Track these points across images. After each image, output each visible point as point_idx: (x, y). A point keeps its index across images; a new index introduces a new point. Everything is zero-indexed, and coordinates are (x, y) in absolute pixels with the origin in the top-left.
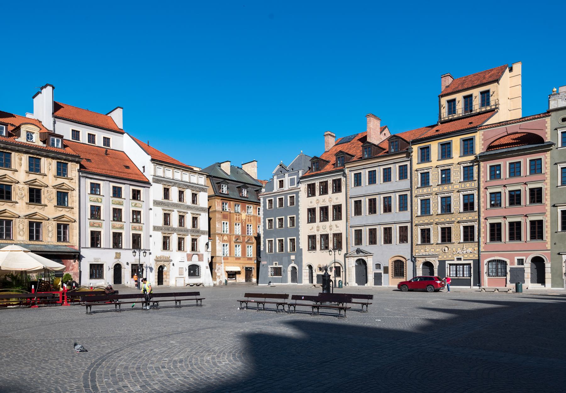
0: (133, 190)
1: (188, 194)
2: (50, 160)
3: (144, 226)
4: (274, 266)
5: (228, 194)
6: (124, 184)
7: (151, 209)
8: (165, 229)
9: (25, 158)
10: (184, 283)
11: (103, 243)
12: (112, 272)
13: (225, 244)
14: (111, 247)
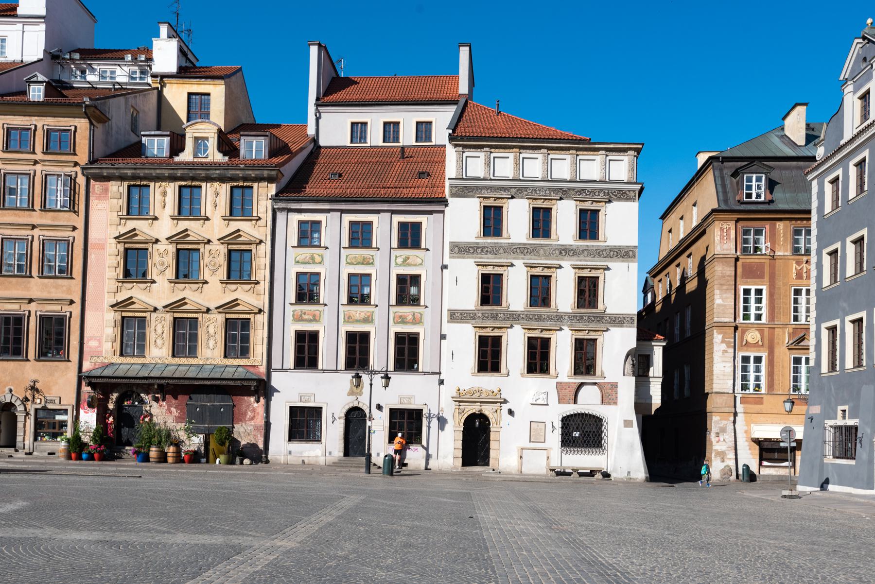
0: (403, 226)
1: (565, 218)
2: (216, 184)
3: (427, 313)
4: (840, 422)
5: (771, 202)
6: (378, 212)
7: (446, 267)
8: (485, 317)
9: (172, 189)
10: (548, 464)
11: (323, 360)
12: (340, 425)
13: (752, 355)
14: (342, 365)
